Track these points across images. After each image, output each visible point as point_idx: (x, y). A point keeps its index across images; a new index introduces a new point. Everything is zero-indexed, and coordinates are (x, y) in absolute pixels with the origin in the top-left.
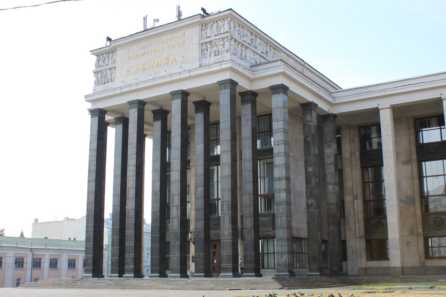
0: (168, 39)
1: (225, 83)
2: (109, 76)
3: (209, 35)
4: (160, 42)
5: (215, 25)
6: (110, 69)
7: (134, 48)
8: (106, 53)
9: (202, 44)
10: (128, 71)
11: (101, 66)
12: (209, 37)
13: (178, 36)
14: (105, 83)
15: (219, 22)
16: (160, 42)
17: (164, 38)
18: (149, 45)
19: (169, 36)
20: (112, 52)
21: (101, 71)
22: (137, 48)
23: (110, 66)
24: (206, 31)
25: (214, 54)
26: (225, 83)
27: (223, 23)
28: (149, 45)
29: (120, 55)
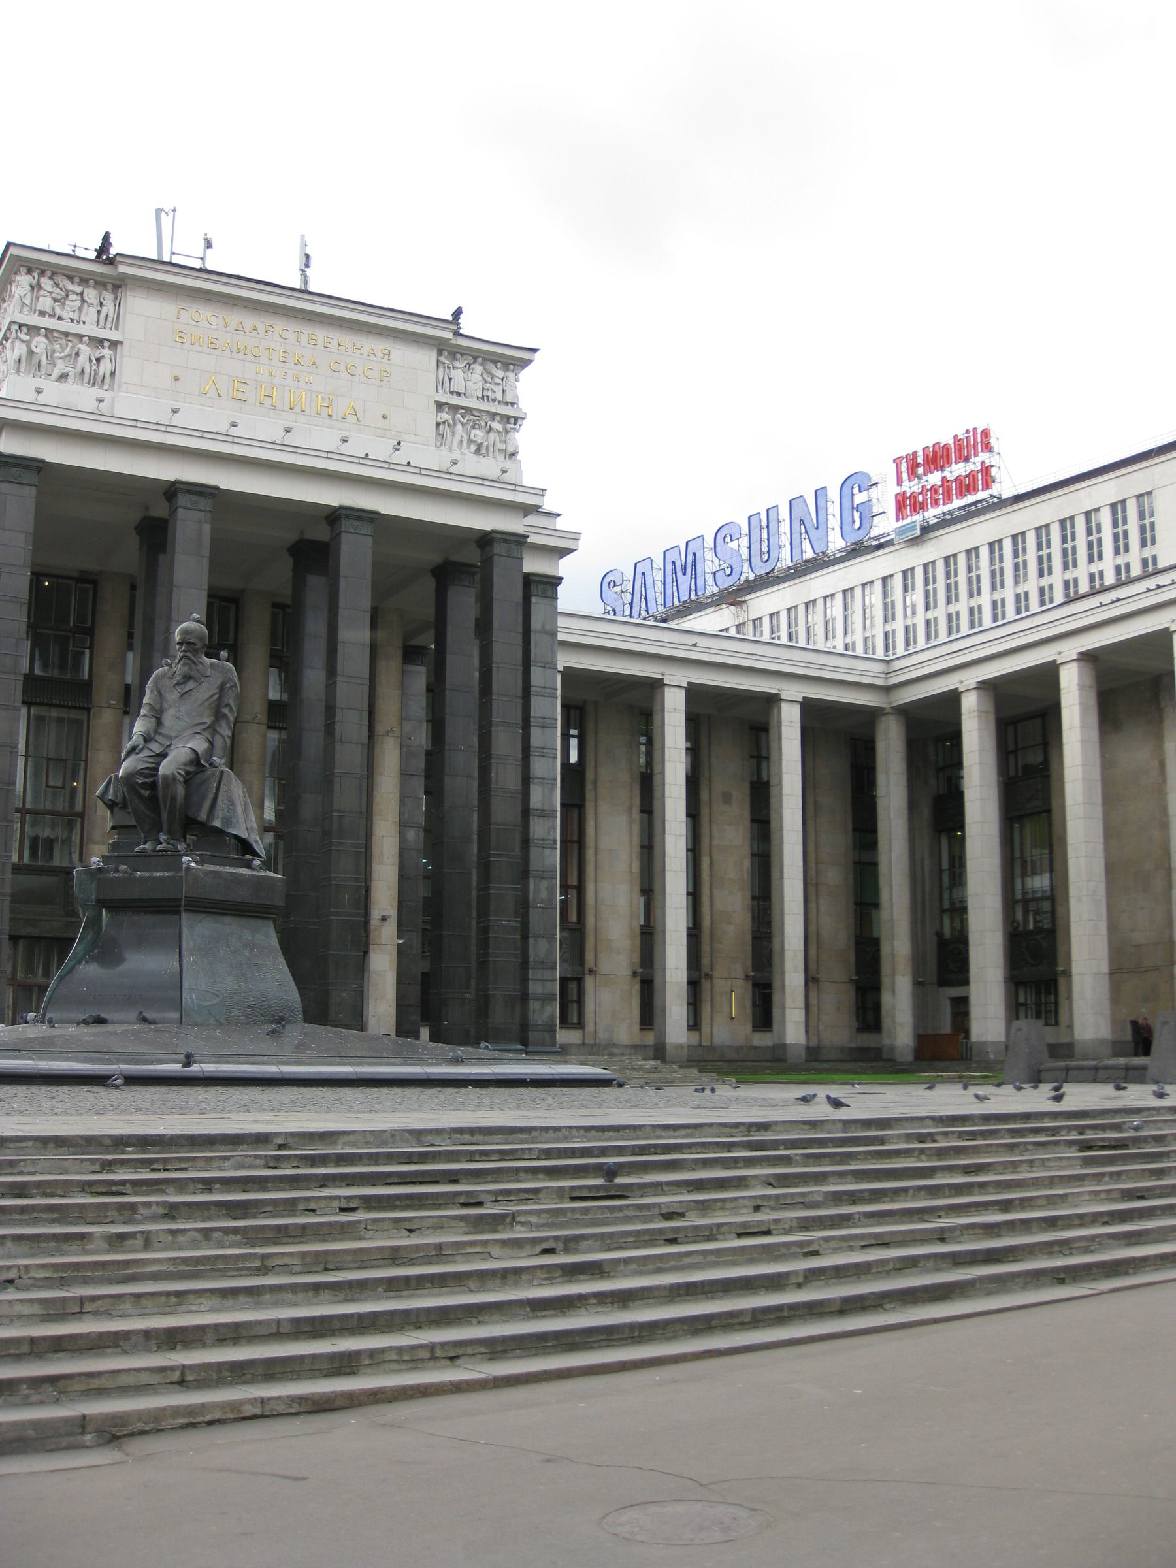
0: (334, 344)
1: (510, 542)
2: (82, 360)
3: (458, 386)
4: (304, 339)
5: (478, 368)
7: (206, 316)
8: (71, 279)
9: (440, 406)
10: (176, 379)
11: (42, 313)
12: (459, 394)
13: (366, 350)
14: (63, 377)
15: (491, 367)
16: (304, 339)
17: (322, 334)
18: (261, 328)
19: (339, 337)
20: (97, 283)
21: (49, 331)
22: (213, 320)
23: (91, 330)
24: (453, 373)
25: (473, 448)
26: (510, 542)
27: (500, 374)
28: (261, 328)
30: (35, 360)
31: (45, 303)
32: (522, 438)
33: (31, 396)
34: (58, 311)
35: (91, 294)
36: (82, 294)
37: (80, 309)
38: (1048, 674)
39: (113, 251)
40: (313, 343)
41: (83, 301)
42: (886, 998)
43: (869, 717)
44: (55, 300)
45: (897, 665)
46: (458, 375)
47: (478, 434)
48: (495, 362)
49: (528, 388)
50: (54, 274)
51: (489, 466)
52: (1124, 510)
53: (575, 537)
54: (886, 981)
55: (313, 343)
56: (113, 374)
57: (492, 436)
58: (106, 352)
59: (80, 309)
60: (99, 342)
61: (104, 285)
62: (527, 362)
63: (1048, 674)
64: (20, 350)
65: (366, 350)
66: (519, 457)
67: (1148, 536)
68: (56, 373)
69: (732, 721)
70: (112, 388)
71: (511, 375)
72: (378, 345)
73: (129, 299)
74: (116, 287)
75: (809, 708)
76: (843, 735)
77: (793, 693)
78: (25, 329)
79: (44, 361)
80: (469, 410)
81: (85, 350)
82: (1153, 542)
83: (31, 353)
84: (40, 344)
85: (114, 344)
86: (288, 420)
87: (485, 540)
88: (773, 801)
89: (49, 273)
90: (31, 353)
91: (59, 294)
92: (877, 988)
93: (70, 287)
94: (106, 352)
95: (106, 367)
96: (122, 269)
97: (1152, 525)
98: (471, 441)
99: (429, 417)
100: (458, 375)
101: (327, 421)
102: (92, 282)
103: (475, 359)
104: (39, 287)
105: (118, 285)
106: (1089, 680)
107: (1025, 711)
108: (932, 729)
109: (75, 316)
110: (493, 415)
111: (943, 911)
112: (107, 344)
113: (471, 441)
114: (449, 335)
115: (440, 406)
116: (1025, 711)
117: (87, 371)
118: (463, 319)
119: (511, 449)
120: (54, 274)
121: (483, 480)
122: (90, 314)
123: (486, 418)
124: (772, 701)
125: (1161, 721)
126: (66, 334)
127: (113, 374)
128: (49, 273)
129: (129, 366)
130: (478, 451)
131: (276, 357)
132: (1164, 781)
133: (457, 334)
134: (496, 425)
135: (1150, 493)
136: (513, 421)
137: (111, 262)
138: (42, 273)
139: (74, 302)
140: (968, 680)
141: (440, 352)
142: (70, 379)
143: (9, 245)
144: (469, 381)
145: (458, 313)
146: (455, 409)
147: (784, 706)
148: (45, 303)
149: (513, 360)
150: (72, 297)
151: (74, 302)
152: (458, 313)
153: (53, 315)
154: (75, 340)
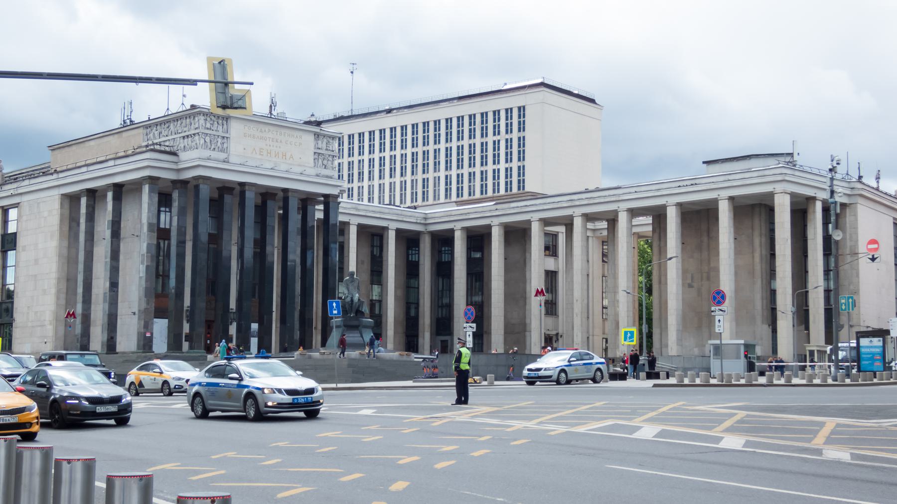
2: (219, 144)
31: (208, 125)
40: (281, 134)
42: (420, 340)
43: (418, 233)
45: (430, 216)
46: (320, 142)
47: (325, 162)
52: (511, 112)
54: (420, 334)
55: (281, 134)
64: (202, 141)
67: (522, 127)
69: (373, 237)
72: (300, 133)
75: (399, 232)
76: (409, 241)
77: (393, 226)
81: (220, 140)
82: (524, 130)
87: (326, 196)
88: (384, 267)
92: (417, 336)
95: (225, 145)
97: (524, 121)
106: (502, 232)
107: (478, 240)
108: (443, 240)
111: (439, 307)
116: (478, 240)
121: (327, 177)
124: (386, 229)
140: (458, 226)
147: (390, 231)
148: (208, 125)
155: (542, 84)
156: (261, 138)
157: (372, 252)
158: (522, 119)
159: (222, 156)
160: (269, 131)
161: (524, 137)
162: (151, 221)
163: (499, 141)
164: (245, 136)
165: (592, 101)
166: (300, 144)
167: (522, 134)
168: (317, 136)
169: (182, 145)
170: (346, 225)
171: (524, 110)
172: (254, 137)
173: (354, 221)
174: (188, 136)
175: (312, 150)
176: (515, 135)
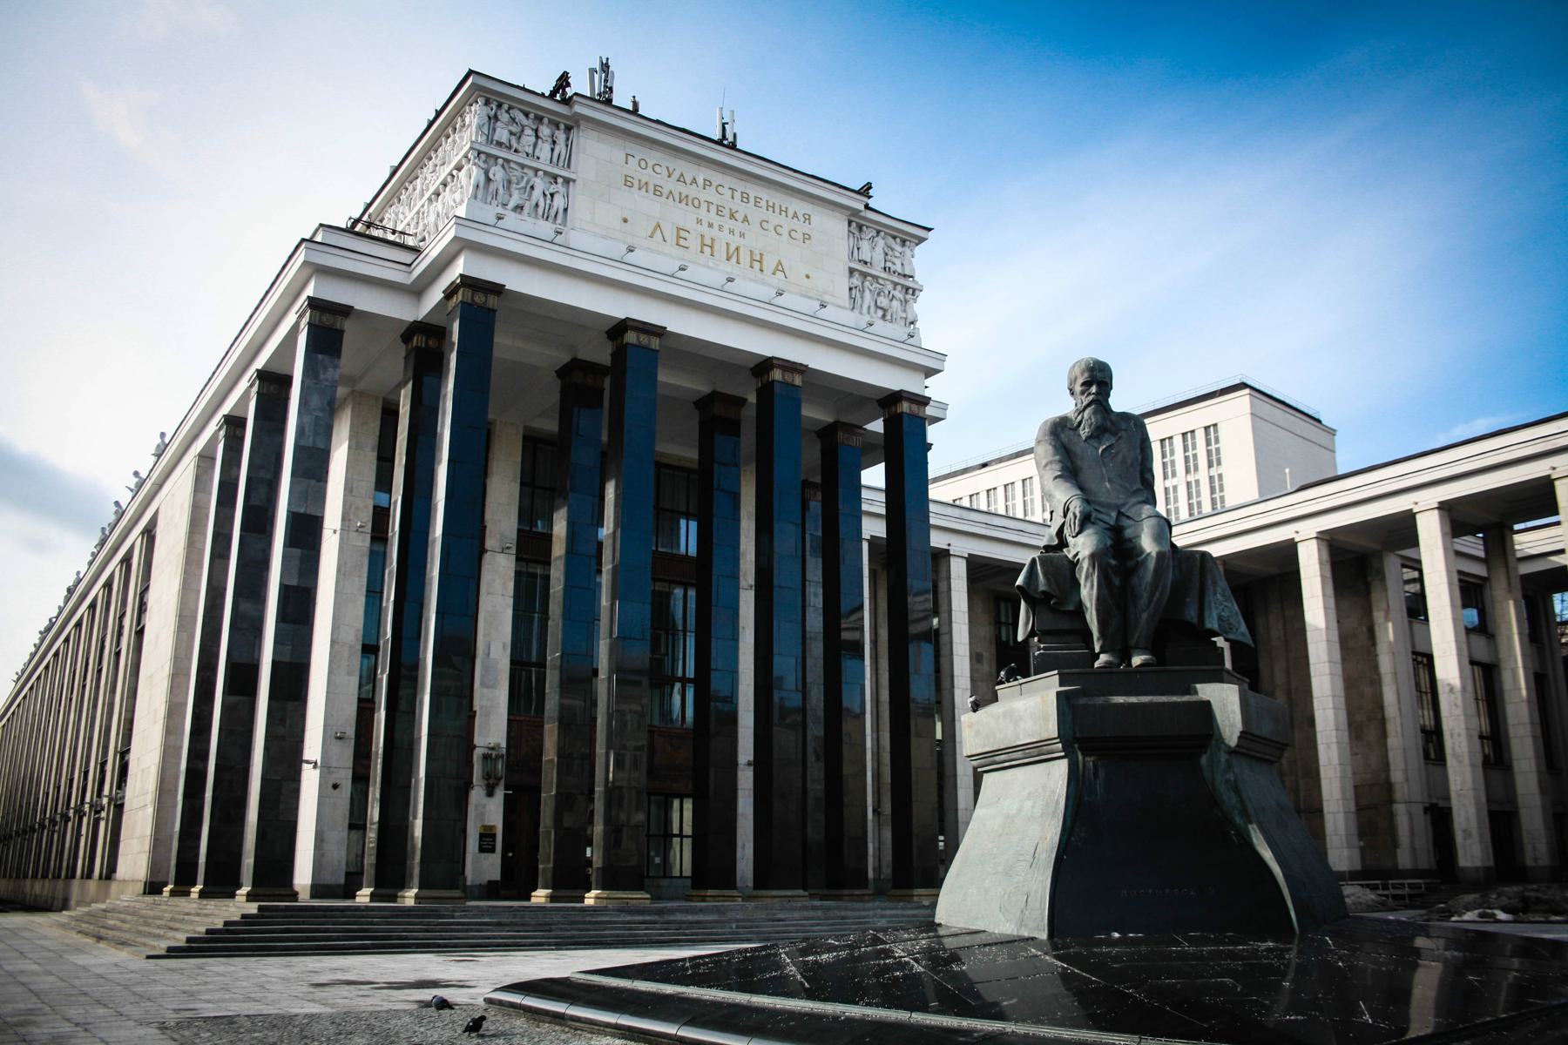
2: (537, 194)
4: (737, 195)
5: (880, 242)
6: (546, 173)
8: (526, 115)
10: (625, 221)
13: (791, 213)
15: (890, 240)
16: (737, 195)
18: (700, 181)
20: (550, 121)
21: (507, 161)
22: (657, 169)
23: (543, 165)
25: (880, 313)
27: (898, 248)
28: (700, 181)
29: (594, 155)
30: (492, 187)
32: (919, 307)
33: (492, 221)
34: (515, 145)
35: (545, 131)
36: (536, 131)
37: (535, 145)
38: (1288, 551)
39: (569, 92)
41: (537, 137)
44: (511, 133)
47: (883, 301)
48: (894, 238)
49: (921, 261)
50: (510, 108)
51: (897, 330)
53: (944, 407)
55: (745, 198)
56: (566, 210)
57: (896, 304)
58: (560, 187)
59: (535, 145)
60: (555, 177)
61: (557, 126)
62: (921, 240)
63: (1288, 551)
65: (791, 213)
66: (918, 325)
68: (512, 204)
70: (564, 223)
71: (906, 249)
72: (801, 207)
73: (582, 140)
74: (568, 129)
78: (483, 157)
79: (501, 191)
80: (875, 278)
81: (540, 184)
82: (1219, 463)
83: (488, 180)
84: (497, 173)
85: (567, 181)
86: (730, 268)
87: (890, 401)
89: (506, 107)
90: (488, 180)
91: (514, 129)
93: (525, 121)
94: (560, 187)
95: (559, 202)
96: (578, 109)
97: (1218, 450)
98: (877, 307)
99: (843, 283)
100: (865, 245)
101: (759, 275)
102: (546, 121)
103: (878, 232)
104: (496, 118)
105: (570, 126)
109: (530, 150)
110: (896, 284)
112: (560, 180)
113: (877, 307)
114: (862, 207)
115: (852, 271)
117: (542, 204)
118: (871, 192)
119: (910, 318)
120: (510, 108)
122: (544, 150)
123: (890, 287)
125: (1368, 593)
126: (523, 166)
127: (566, 210)
128: (506, 107)
129: (581, 204)
130: (884, 316)
131: (713, 209)
132: (1374, 644)
133: (867, 207)
134: (898, 294)
135: (1215, 425)
136: (911, 291)
137: (567, 101)
138: (500, 106)
139: (529, 138)
141: (850, 223)
142: (526, 210)
143: (471, 72)
144: (873, 251)
145: (869, 186)
146: (864, 275)
148: (502, 134)
149: (909, 236)
150: (528, 131)
151: (529, 138)
152: (869, 186)
153: (510, 147)
154: (531, 173)
155: (1243, 386)
156: (682, 199)
157: (998, 637)
158: (1213, 447)
159: (546, 229)
160: (707, 183)
161: (1220, 476)
162: (303, 443)
163: (1175, 488)
164: (628, 182)
165: (1319, 421)
166: (807, 237)
167: (1214, 472)
168: (858, 223)
169: (432, 218)
170: (942, 556)
171: (1216, 431)
172: (657, 191)
173: (961, 548)
174: (445, 184)
175: (842, 263)
176: (1203, 474)
